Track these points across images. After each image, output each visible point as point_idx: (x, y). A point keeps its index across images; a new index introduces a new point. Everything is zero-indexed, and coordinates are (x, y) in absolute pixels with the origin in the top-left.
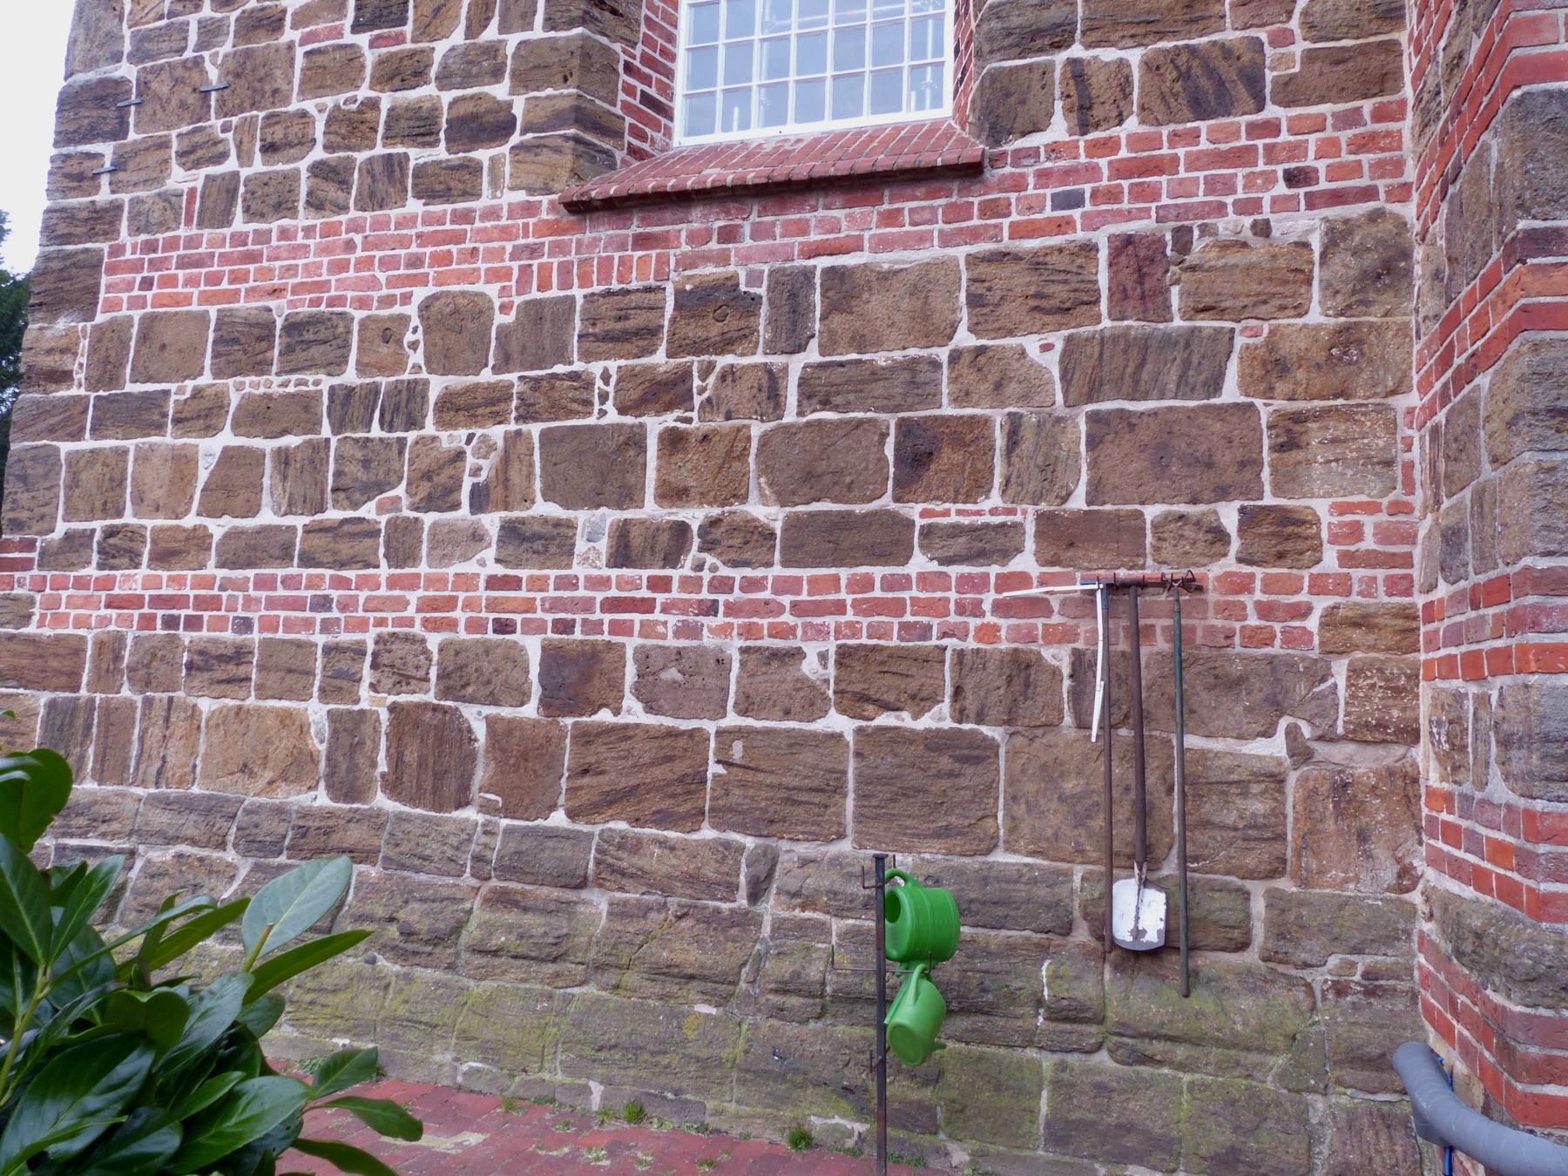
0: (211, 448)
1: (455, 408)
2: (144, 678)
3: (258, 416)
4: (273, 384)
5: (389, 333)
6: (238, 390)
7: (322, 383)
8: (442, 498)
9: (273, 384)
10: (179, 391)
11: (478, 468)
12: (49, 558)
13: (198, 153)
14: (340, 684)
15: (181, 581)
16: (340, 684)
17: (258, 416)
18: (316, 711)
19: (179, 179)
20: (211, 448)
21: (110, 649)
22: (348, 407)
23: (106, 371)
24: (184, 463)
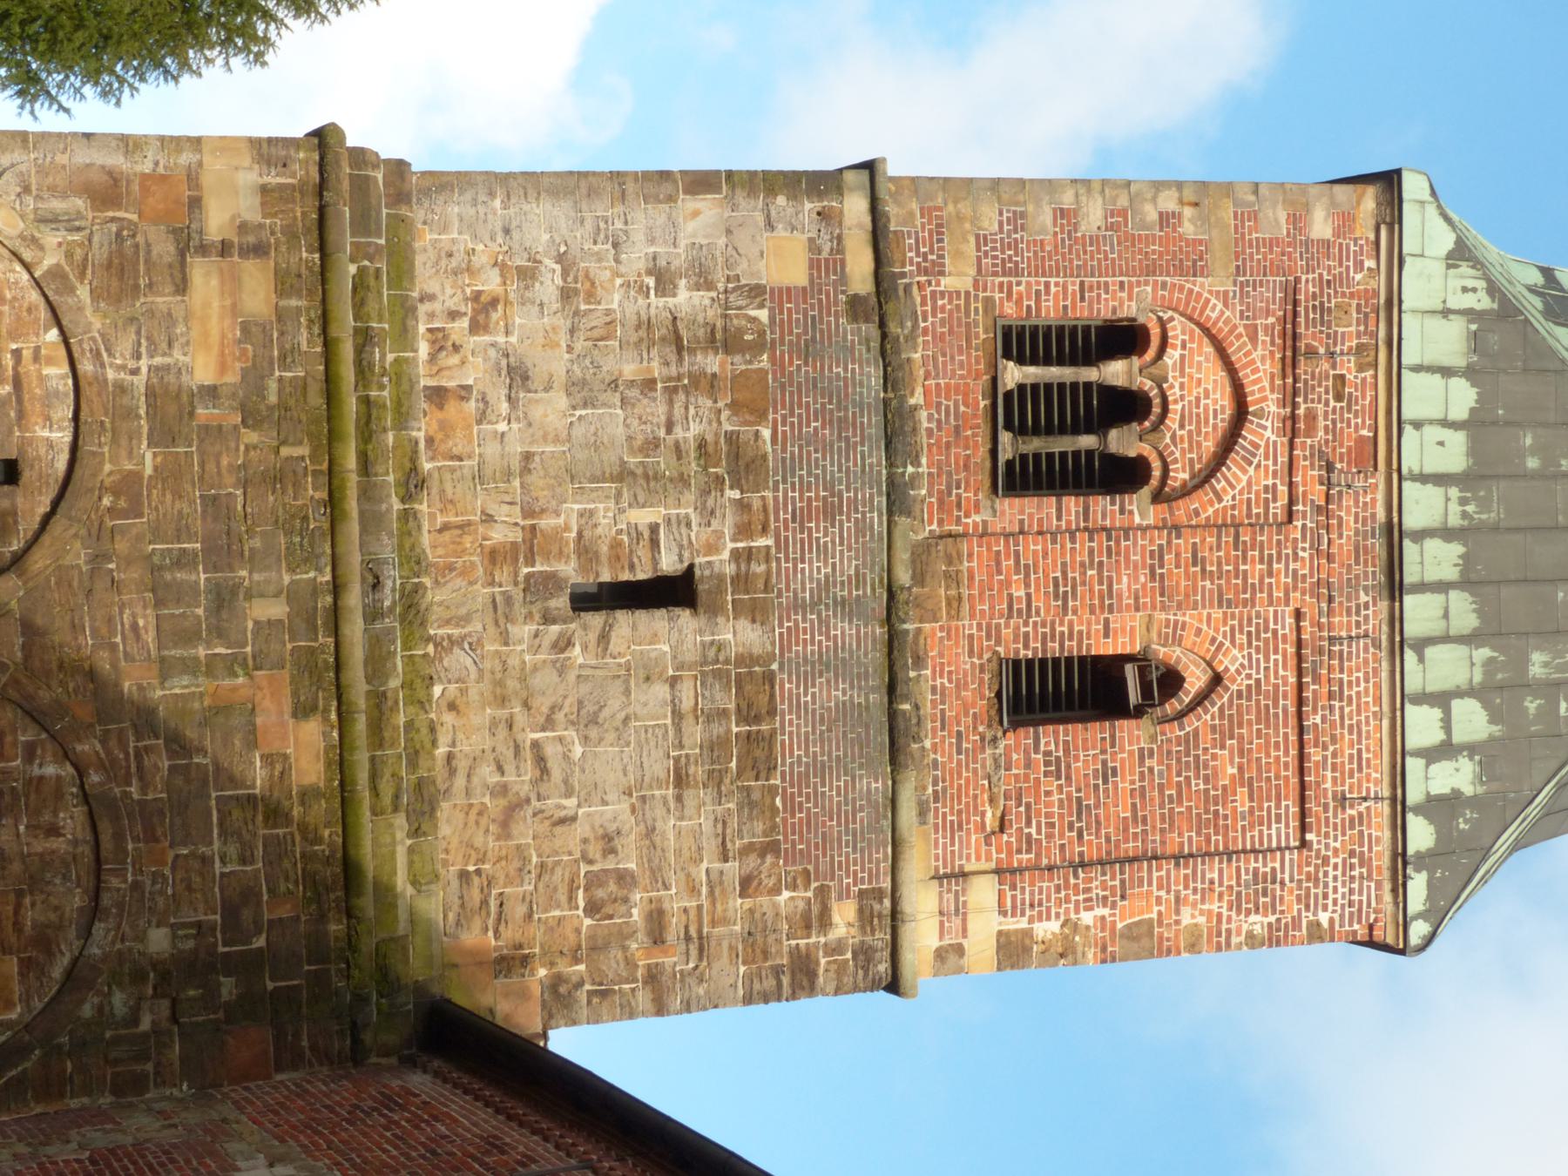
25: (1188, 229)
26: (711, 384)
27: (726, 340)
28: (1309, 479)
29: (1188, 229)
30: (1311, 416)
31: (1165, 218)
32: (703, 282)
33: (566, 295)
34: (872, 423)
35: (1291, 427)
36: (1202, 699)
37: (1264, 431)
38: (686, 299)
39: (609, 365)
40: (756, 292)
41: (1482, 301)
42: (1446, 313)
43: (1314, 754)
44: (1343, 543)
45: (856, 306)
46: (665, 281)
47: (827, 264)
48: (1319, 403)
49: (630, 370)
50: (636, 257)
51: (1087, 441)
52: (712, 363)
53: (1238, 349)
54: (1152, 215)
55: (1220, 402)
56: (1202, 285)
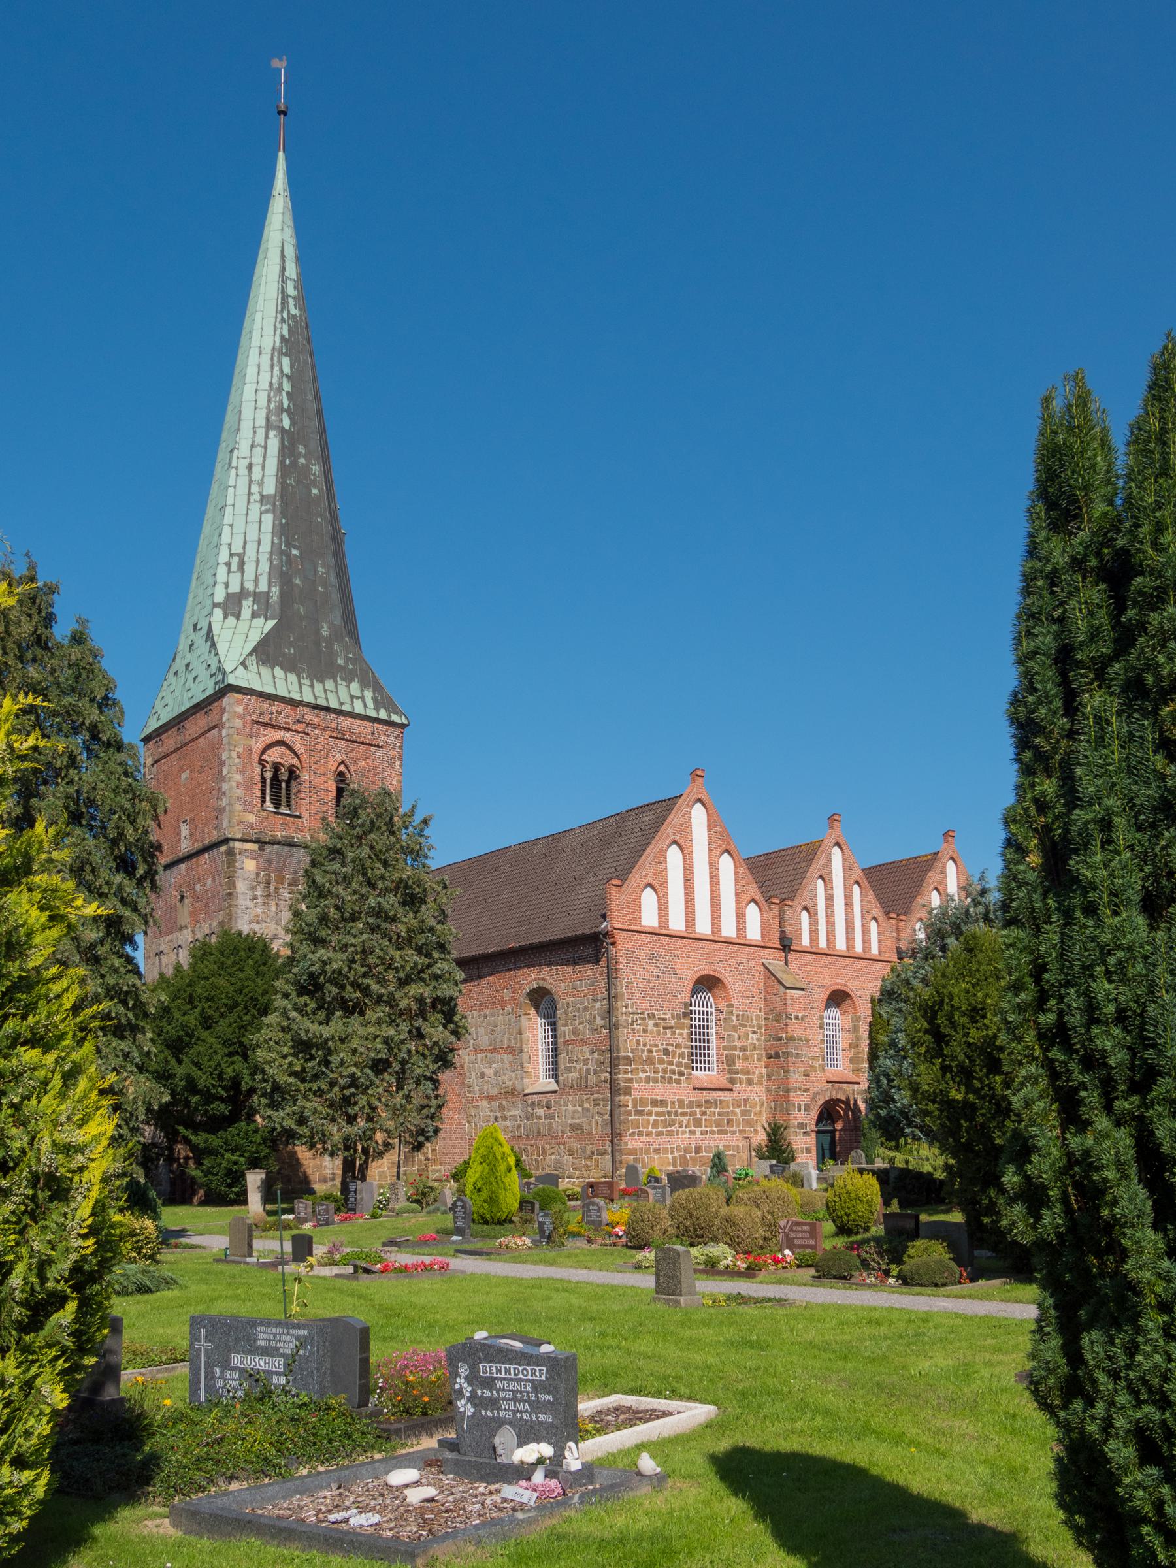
0: (653, 1118)
1: (683, 1114)
2: (646, 1153)
3: (658, 1114)
4: (659, 1109)
5: (673, 1103)
6: (655, 1110)
7: (665, 1110)
8: (681, 1127)
9: (659, 1109)
10: (646, 1110)
11: (685, 1123)
12: (630, 1135)
13: (644, 1071)
14: (672, 1152)
15: (650, 1139)
16: (672, 1152)
17: (658, 1114)
18: (670, 1156)
19: (641, 1075)
20: (653, 1118)
21: (641, 1149)
22: (669, 1113)
23: (635, 1106)
24: (648, 1121)
25: (241, 750)
26: (277, 888)
27: (268, 883)
28: (300, 727)
29: (241, 750)
30: (286, 723)
31: (239, 757)
32: (254, 888)
33: (258, 922)
34: (287, 848)
35: (289, 730)
36: (346, 766)
37: (287, 736)
38: (259, 893)
39: (273, 914)
40: (258, 874)
41: (254, 658)
42: (259, 673)
43: (362, 739)
44: (316, 721)
45: (261, 849)
46: (255, 898)
47: (252, 855)
48: (282, 720)
49: (274, 908)
50: (250, 904)
51: (284, 785)
52: (272, 888)
53: (269, 742)
54: (237, 760)
55: (278, 749)
56: (254, 748)
